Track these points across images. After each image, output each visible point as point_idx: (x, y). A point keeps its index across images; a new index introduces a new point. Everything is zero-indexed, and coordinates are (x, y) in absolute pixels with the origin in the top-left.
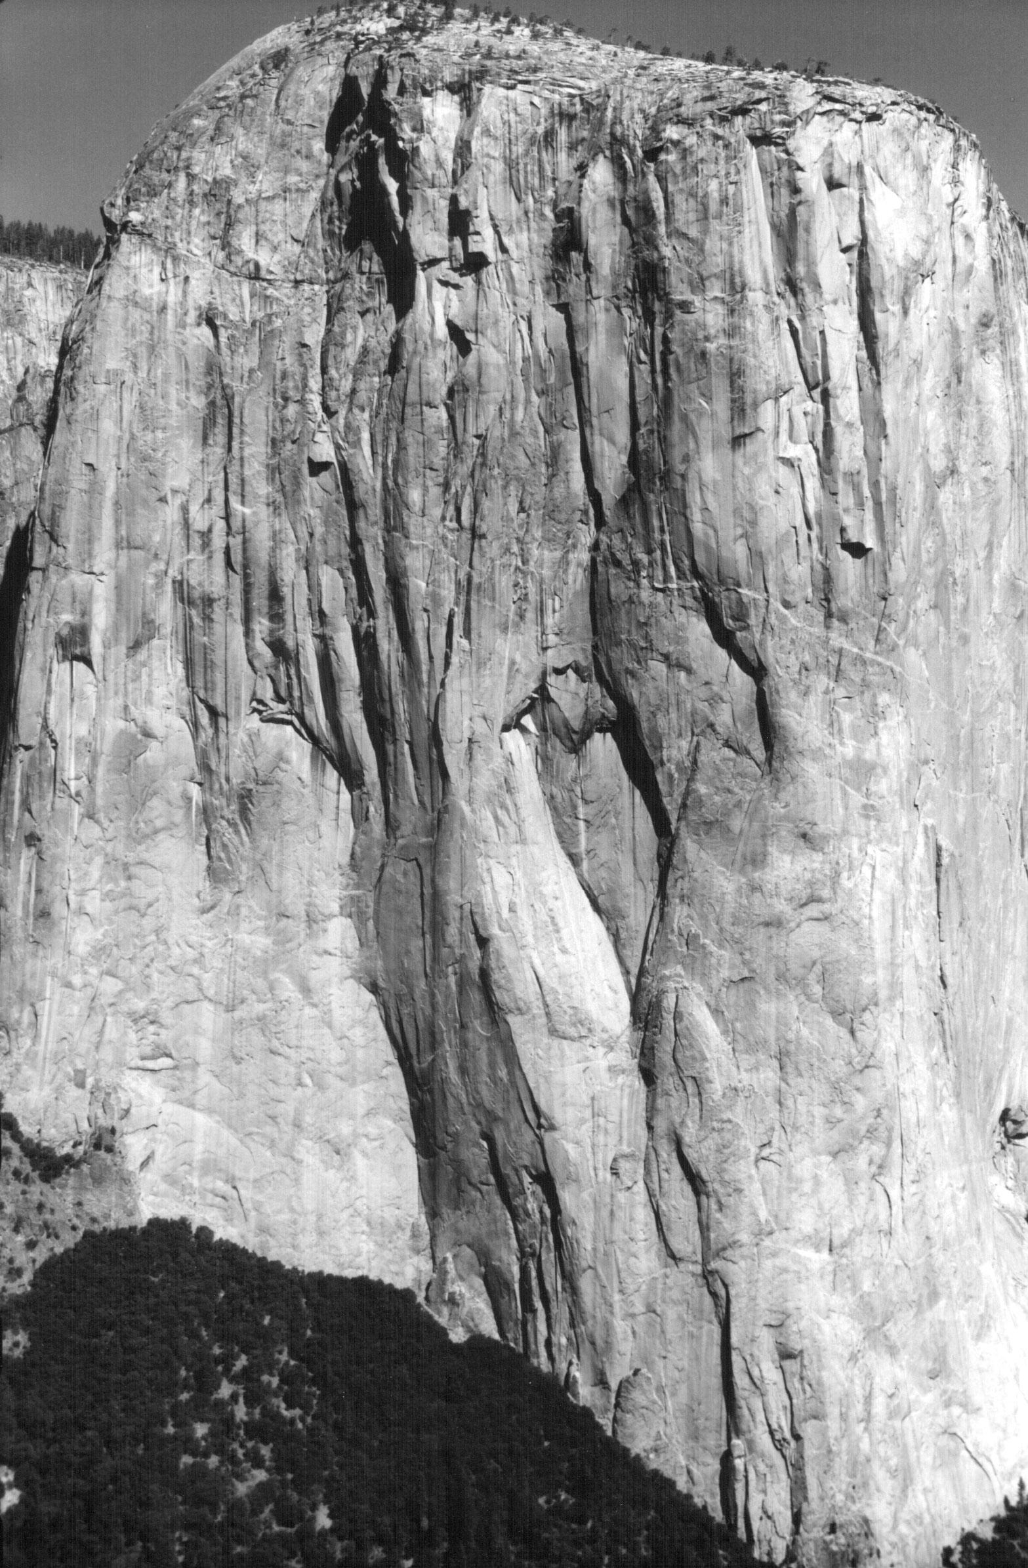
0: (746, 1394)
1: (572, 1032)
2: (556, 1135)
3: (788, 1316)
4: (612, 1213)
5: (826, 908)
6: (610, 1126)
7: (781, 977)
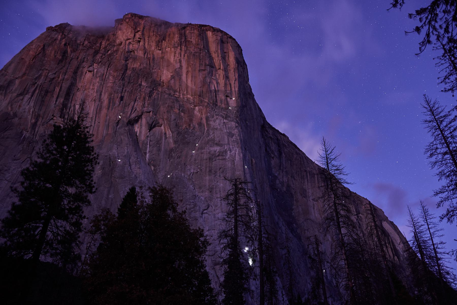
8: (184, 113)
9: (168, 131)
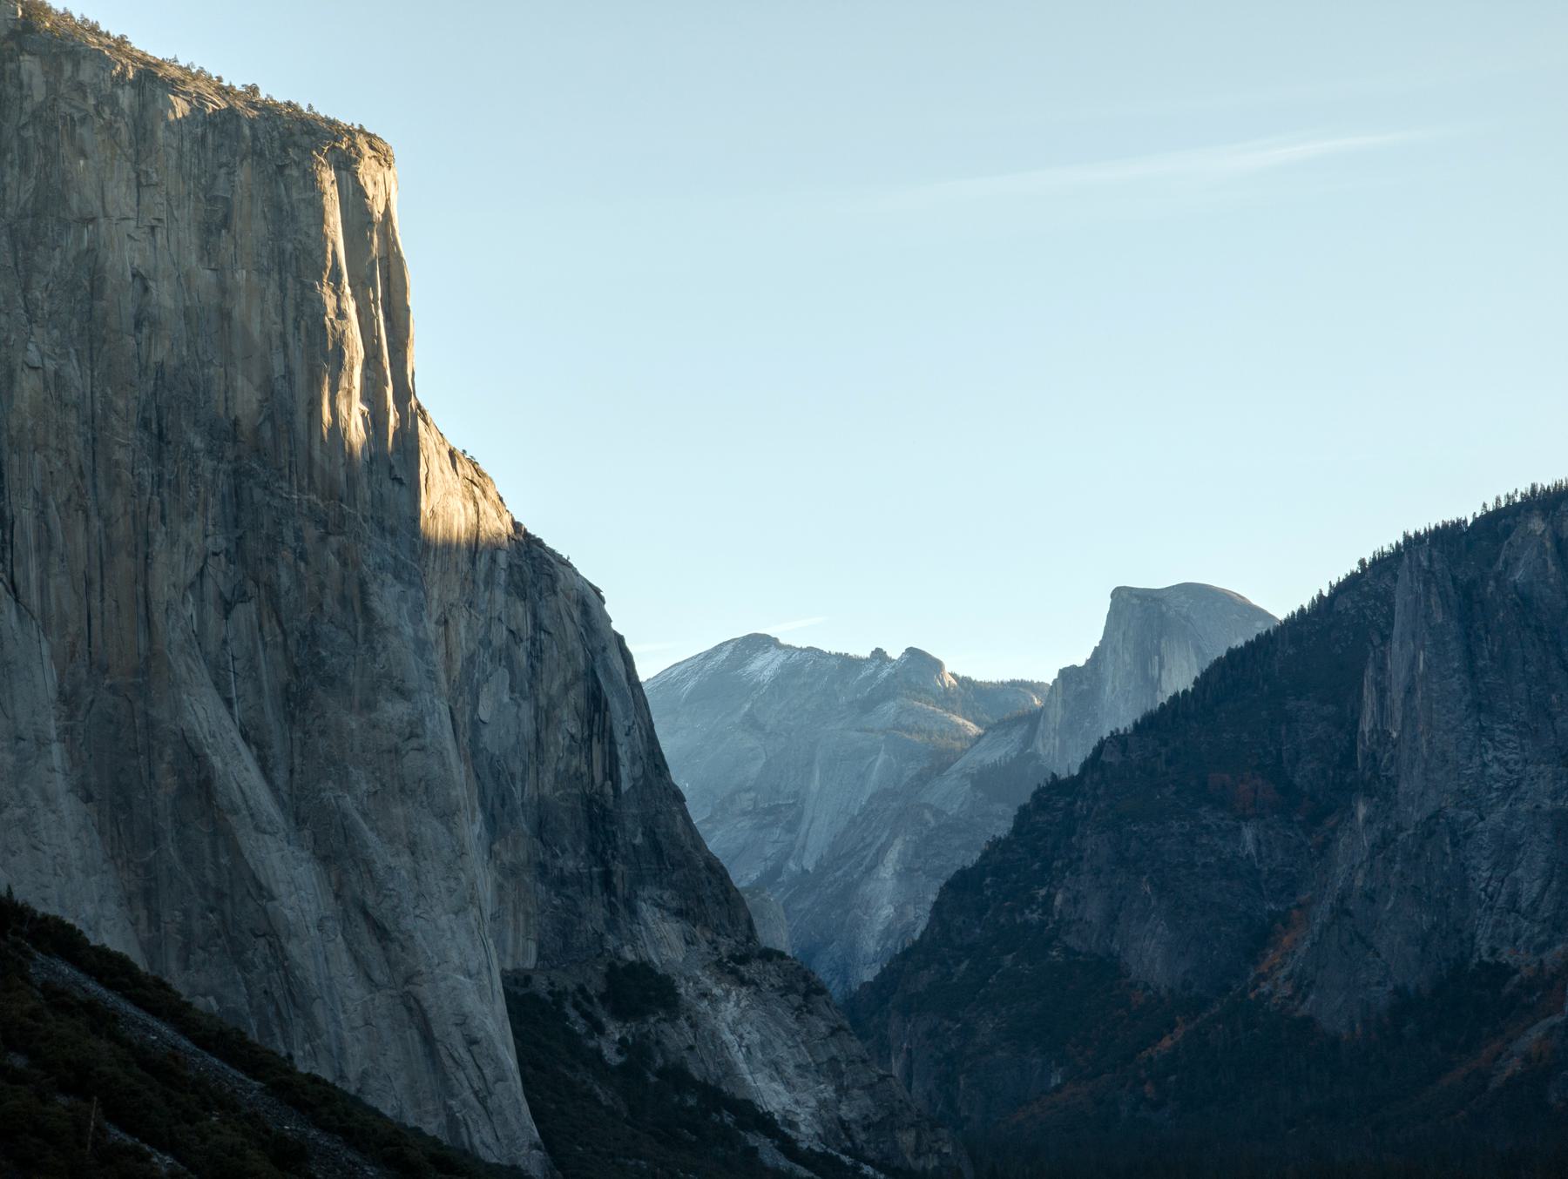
0: (453, 1070)
1: (269, 828)
2: (276, 903)
3: (467, 1017)
4: (326, 959)
5: (422, 741)
6: (310, 897)
7: (402, 790)
8: (307, 563)
9: (270, 622)
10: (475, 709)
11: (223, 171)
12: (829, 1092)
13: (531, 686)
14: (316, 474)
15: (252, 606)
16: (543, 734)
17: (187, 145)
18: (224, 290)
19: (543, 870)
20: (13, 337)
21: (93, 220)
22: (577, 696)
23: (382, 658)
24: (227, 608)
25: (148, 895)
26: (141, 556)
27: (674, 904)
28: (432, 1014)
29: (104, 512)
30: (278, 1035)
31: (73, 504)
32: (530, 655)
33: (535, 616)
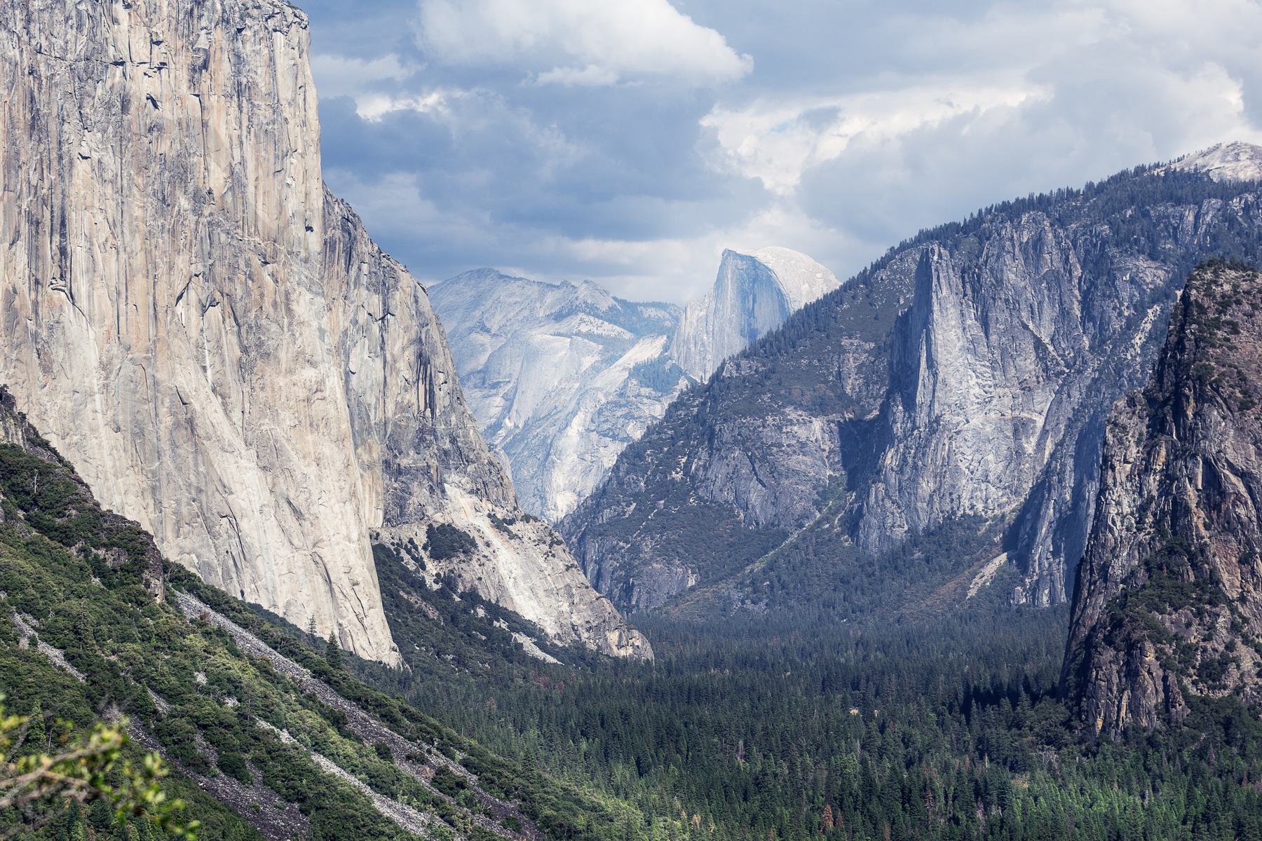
1: (230, 450)
2: (233, 496)
5: (324, 394)
7: (311, 425)
10: (347, 364)
11: (204, 31)
12: (565, 607)
13: (382, 349)
14: (260, 228)
15: (218, 309)
16: (388, 379)
17: (182, 16)
18: (203, 109)
19: (387, 463)
20: (72, 137)
21: (122, 64)
22: (410, 355)
23: (299, 342)
24: (204, 309)
25: (154, 489)
26: (151, 277)
27: (469, 486)
28: (329, 567)
29: (128, 249)
30: (235, 579)
31: (109, 244)
32: (381, 328)
33: (384, 304)
